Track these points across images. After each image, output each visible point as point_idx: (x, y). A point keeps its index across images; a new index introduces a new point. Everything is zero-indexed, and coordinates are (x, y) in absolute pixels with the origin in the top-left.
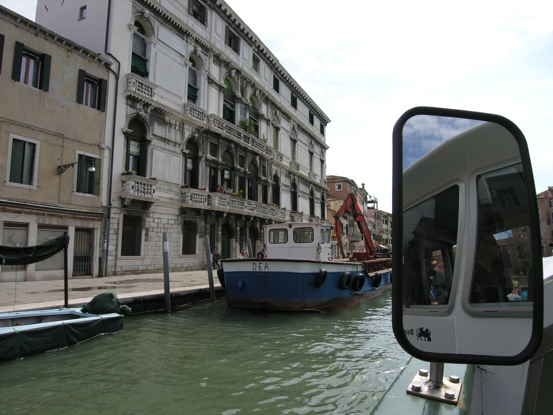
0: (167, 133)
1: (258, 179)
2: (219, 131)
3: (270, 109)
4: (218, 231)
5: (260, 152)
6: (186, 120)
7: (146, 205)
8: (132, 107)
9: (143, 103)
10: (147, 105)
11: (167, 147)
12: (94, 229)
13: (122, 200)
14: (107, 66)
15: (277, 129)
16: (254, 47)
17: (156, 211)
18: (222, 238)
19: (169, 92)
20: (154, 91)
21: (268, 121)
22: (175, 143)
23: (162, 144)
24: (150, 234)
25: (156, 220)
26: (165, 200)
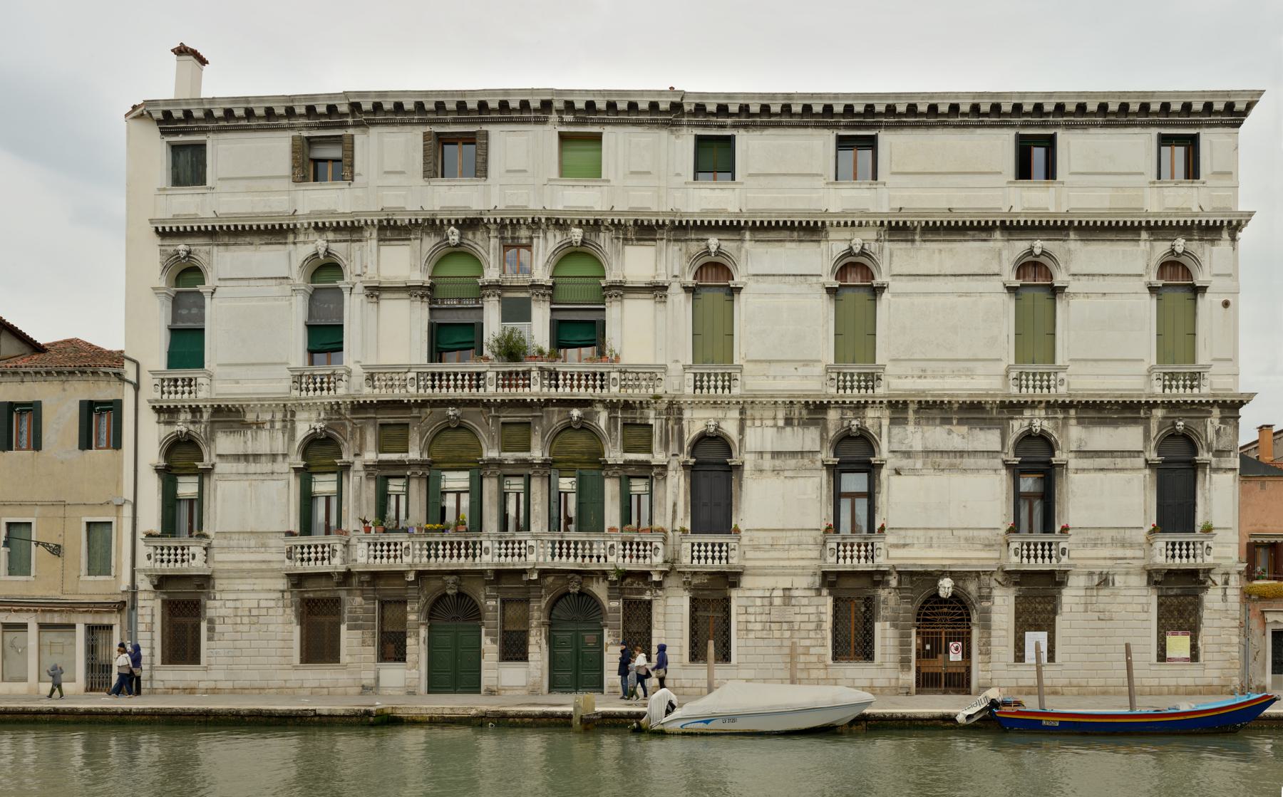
0: (249, 443)
2: (397, 394)
7: (205, 582)
8: (167, 423)
10: (195, 410)
11: (253, 467)
22: (274, 457)
23: (241, 467)
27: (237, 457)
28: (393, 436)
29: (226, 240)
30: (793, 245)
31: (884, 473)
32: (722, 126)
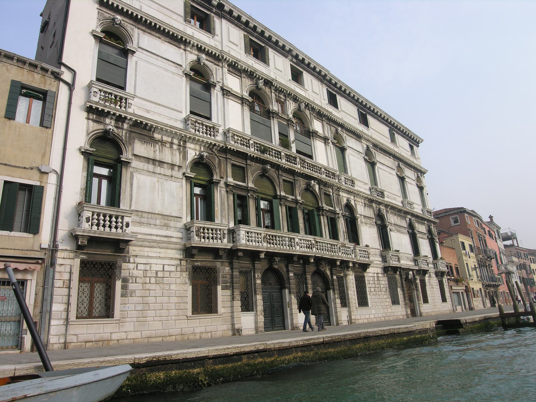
0: (157, 153)
1: (319, 209)
2: (243, 149)
3: (326, 126)
4: (255, 279)
5: (315, 175)
6: (186, 136)
9: (114, 117)
10: (120, 119)
11: (158, 170)
12: (27, 280)
13: (75, 237)
14: (57, 77)
15: (342, 150)
16: (290, 57)
17: (141, 253)
18: (263, 288)
19: (159, 105)
20: (130, 101)
21: (325, 140)
22: (172, 166)
23: (151, 167)
24: (131, 286)
25: (141, 267)
26: (158, 238)
27: (148, 160)
28: (240, 172)
29: (144, 28)
30: (354, 140)
31: (388, 230)
32: (333, 90)
